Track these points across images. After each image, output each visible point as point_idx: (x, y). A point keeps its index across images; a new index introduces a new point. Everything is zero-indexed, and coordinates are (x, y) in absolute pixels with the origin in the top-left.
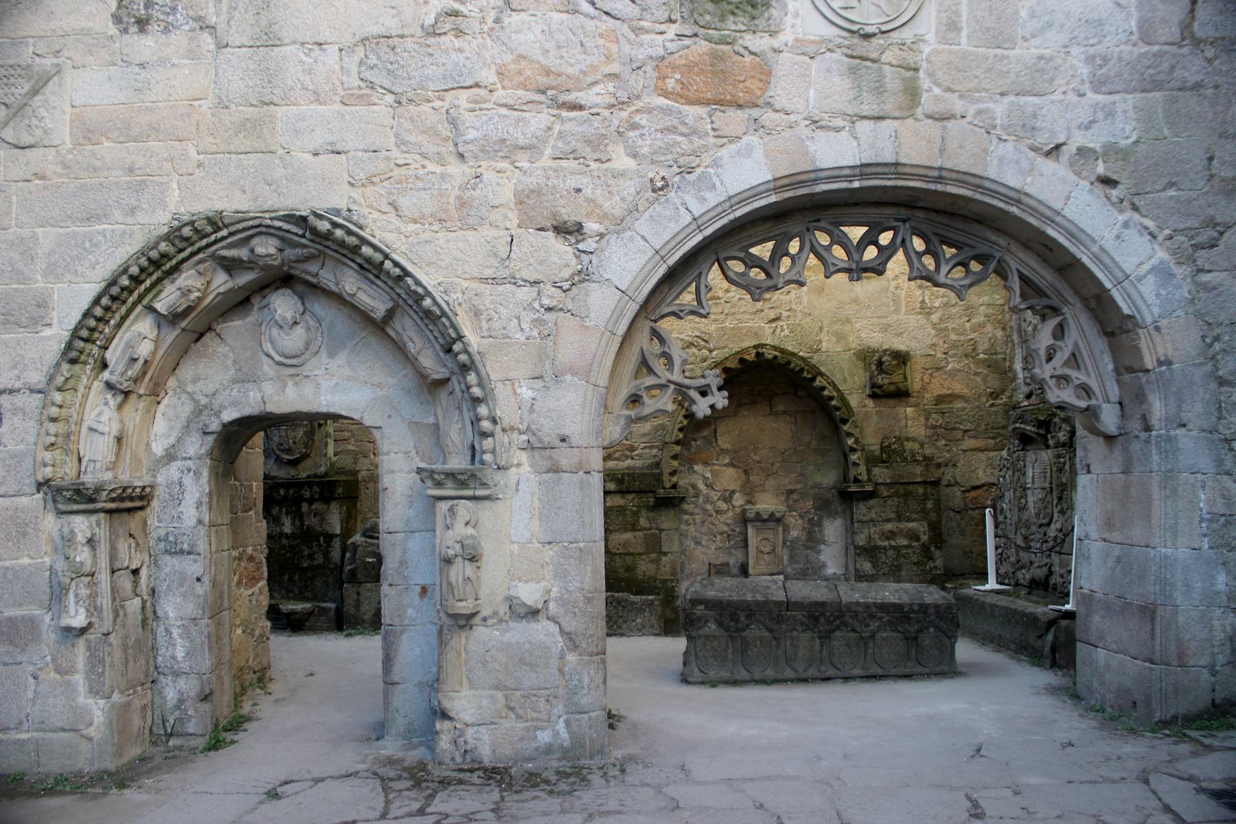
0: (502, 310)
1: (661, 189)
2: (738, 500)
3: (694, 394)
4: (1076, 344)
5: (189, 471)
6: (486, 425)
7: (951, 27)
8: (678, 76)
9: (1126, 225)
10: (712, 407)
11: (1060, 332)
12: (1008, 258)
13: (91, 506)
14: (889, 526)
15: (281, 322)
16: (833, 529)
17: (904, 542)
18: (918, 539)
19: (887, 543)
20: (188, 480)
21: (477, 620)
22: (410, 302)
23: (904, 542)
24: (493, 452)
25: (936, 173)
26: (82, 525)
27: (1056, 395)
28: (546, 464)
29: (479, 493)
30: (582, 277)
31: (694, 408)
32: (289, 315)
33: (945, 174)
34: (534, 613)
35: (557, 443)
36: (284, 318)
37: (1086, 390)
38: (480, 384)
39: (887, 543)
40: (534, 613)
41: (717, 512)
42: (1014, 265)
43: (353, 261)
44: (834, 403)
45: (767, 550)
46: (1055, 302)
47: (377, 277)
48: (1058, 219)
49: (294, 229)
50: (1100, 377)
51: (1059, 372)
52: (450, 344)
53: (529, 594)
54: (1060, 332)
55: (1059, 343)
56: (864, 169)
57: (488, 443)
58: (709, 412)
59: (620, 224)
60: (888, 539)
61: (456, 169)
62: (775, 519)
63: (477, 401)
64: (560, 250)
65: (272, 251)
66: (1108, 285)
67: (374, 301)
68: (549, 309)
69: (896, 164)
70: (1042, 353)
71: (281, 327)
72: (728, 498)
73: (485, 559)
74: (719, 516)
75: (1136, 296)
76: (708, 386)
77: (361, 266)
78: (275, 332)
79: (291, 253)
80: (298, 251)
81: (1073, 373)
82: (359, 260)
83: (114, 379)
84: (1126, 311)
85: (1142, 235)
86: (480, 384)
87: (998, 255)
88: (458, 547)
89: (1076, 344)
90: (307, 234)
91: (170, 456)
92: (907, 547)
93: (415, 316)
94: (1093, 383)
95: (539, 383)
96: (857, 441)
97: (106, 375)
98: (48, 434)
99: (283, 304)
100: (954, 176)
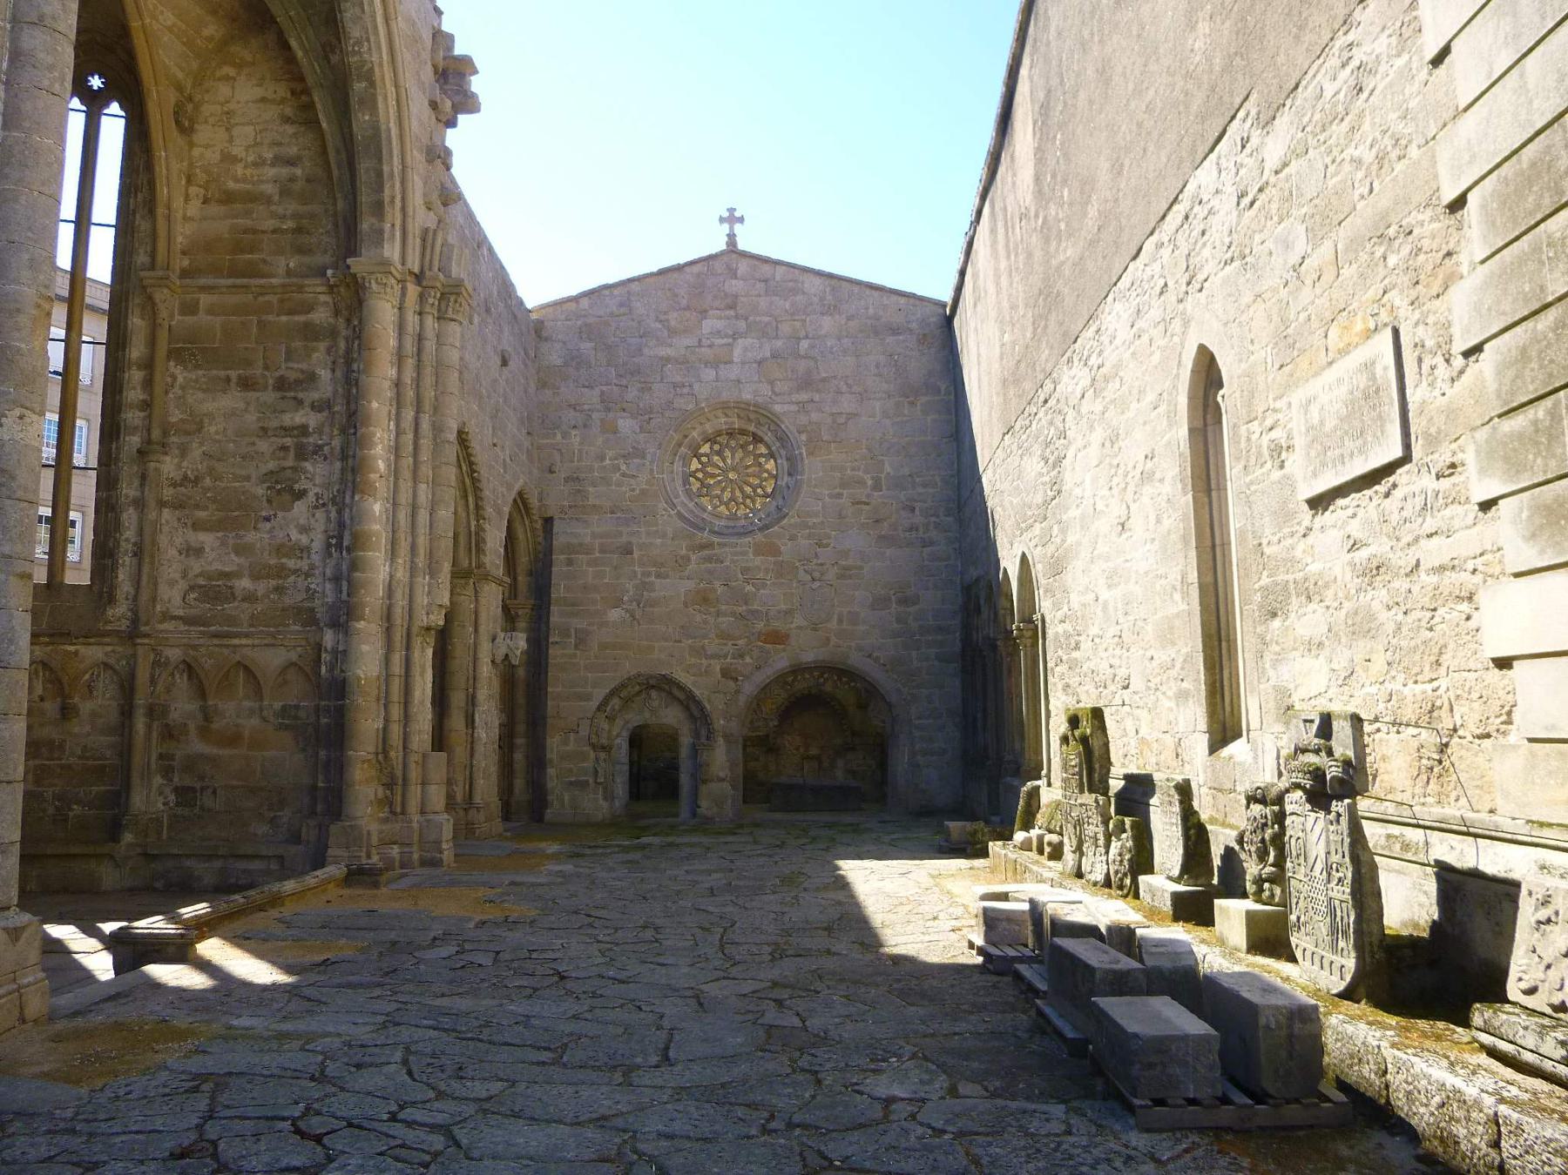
2: (802, 750)
7: (840, 621)
16: (840, 763)
26: (603, 755)
30: (737, 692)
34: (723, 780)
40: (723, 780)
52: (702, 709)
53: (722, 774)
56: (815, 662)
59: (747, 677)
61: (704, 661)
62: (818, 758)
64: (731, 684)
67: (682, 696)
72: (797, 749)
91: (618, 736)
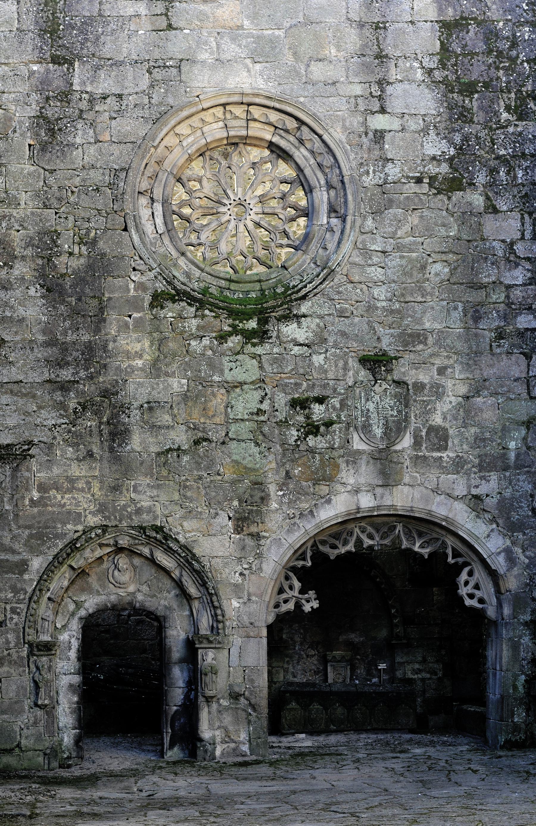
0: (226, 570)
1: (292, 518)
3: (303, 602)
4: (478, 578)
5: (74, 636)
6: (220, 618)
8: (300, 469)
9: (492, 530)
10: (312, 607)
11: (470, 574)
12: (446, 540)
13: (49, 653)
14: (417, 666)
15: (120, 569)
17: (428, 676)
18: (436, 674)
19: (416, 676)
20: (73, 640)
21: (215, 699)
22: (187, 565)
23: (428, 676)
24: (224, 628)
25: (409, 509)
27: (468, 602)
28: (244, 634)
29: (217, 646)
31: (304, 608)
32: (125, 567)
33: (414, 509)
35: (249, 625)
36: (122, 568)
37: (481, 601)
38: (218, 601)
39: (416, 676)
41: (307, 656)
42: (449, 543)
43: (162, 547)
44: (383, 586)
45: (340, 680)
46: (468, 560)
47: (173, 554)
48: (463, 528)
49: (137, 533)
50: (488, 594)
51: (470, 592)
54: (470, 574)
55: (471, 578)
57: (220, 626)
58: (310, 610)
60: (417, 673)
63: (217, 607)
65: (126, 542)
66: (485, 557)
68: (245, 569)
69: (393, 505)
70: (462, 582)
71: (119, 571)
73: (219, 674)
74: (309, 659)
75: (497, 562)
76: (310, 598)
77: (165, 549)
78: (116, 573)
79: (132, 542)
80: (137, 541)
81: (476, 592)
82: (165, 547)
83: (53, 597)
84: (493, 568)
85: (499, 534)
86: (218, 601)
87: (442, 538)
88: (210, 668)
89: (478, 578)
90: (143, 536)
92: (430, 679)
93: (188, 571)
94: (486, 597)
95: (241, 601)
96: (397, 611)
97: (48, 594)
98: (29, 621)
99: (123, 561)
100: (418, 510)
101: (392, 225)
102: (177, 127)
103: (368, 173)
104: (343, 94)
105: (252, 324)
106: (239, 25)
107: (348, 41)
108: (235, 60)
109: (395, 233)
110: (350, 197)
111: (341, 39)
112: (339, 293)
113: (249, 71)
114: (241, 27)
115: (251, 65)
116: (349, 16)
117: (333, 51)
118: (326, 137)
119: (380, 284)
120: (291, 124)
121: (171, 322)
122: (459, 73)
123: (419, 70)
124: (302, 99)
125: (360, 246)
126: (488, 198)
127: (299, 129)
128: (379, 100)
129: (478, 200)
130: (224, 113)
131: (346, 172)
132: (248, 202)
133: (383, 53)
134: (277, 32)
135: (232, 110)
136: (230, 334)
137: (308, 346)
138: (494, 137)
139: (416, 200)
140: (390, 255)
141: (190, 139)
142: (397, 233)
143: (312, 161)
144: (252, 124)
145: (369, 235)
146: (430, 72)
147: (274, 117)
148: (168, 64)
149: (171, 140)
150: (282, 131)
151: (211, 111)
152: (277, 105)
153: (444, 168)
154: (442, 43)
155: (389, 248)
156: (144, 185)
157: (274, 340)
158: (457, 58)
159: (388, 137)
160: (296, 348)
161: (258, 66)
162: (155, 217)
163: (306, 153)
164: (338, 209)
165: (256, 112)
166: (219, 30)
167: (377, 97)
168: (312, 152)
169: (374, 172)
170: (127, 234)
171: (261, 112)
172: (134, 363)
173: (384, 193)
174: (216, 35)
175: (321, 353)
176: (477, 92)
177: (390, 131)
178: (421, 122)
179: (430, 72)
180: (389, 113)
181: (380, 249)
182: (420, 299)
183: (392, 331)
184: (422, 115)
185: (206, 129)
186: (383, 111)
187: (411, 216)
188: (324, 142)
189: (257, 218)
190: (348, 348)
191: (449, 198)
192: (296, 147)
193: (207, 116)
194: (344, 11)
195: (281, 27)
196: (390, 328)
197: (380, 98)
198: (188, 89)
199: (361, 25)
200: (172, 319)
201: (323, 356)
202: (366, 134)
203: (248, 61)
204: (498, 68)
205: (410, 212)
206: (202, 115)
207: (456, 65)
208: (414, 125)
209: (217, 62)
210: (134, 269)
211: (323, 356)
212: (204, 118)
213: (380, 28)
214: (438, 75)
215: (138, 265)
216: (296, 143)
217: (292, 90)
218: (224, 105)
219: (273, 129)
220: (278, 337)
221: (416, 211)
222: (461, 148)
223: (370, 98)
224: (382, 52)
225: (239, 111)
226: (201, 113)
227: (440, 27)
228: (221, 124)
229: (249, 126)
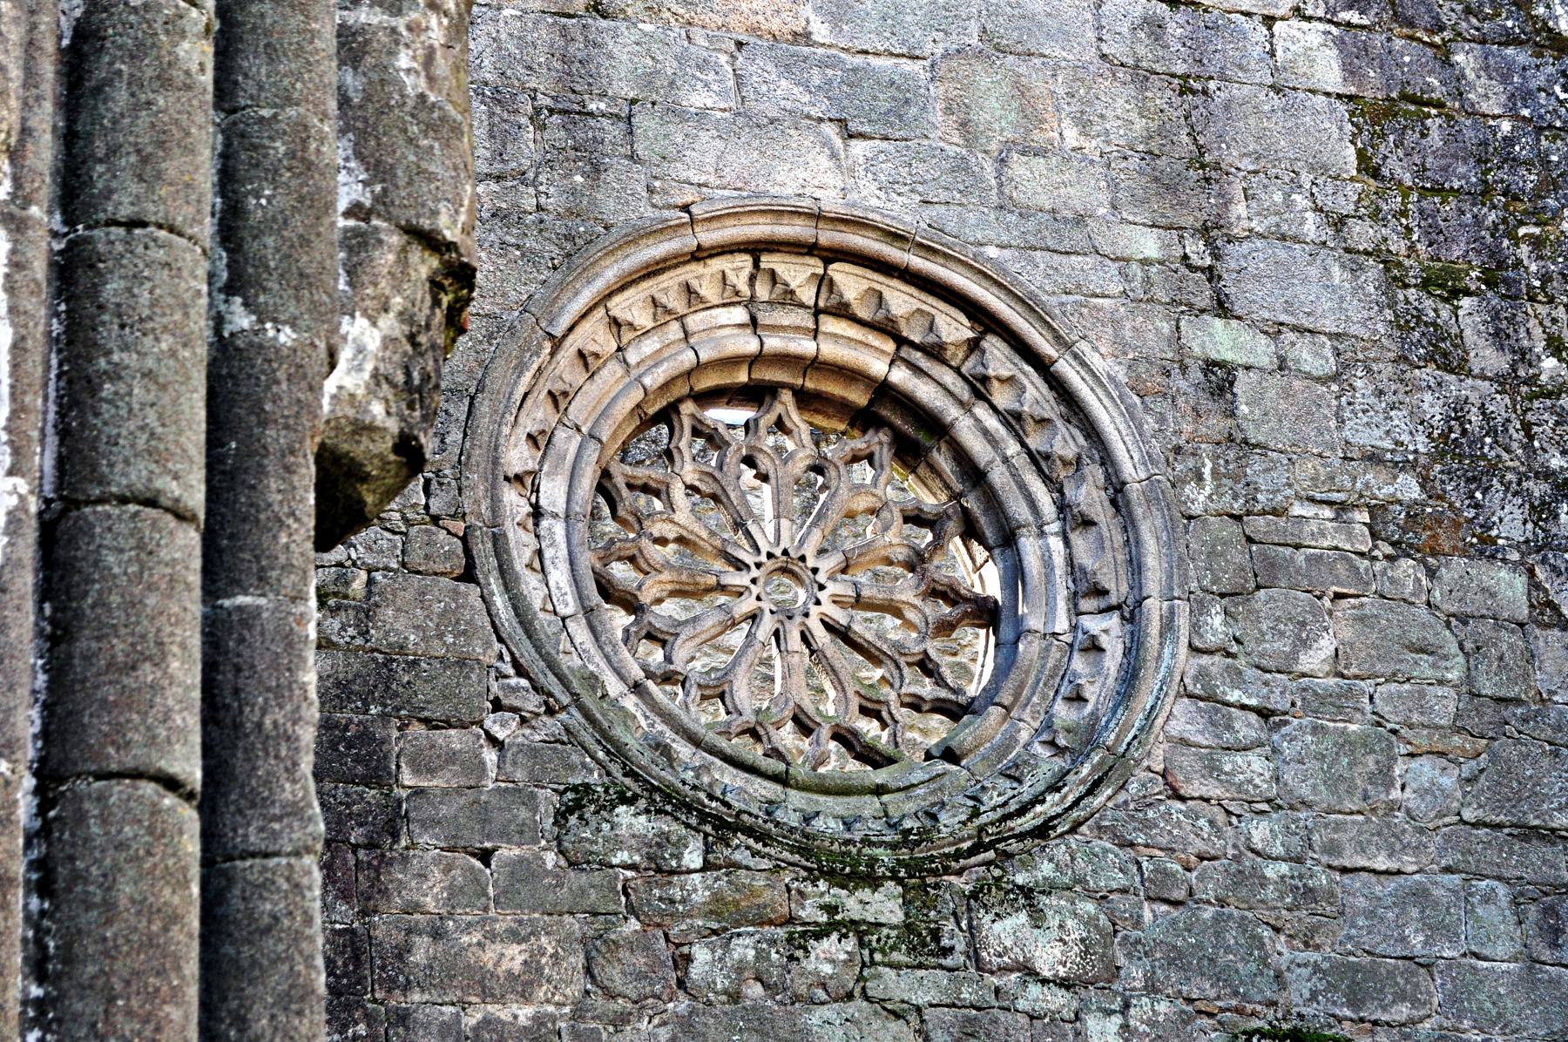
101: (1282, 634)
102: (617, 299)
103: (1199, 478)
104: (1107, 250)
105: (884, 905)
106: (799, 30)
107: (1109, 114)
108: (799, 118)
109: (1293, 657)
110: (1150, 546)
111: (1090, 103)
112: (1148, 825)
113: (834, 156)
114: (803, 37)
115: (838, 142)
116: (1105, 50)
117: (1072, 137)
118: (1066, 368)
119: (1265, 807)
120: (954, 328)
121: (626, 880)
122: (1415, 237)
123: (1310, 215)
124: (992, 252)
125: (1198, 690)
126: (1534, 585)
127: (974, 346)
128: (1210, 280)
129: (1511, 585)
130: (752, 279)
131: (1130, 470)
132: (811, 563)
133: (1208, 158)
134: (908, 66)
135: (780, 269)
136: (821, 933)
137: (1064, 984)
138: (1529, 417)
139: (1341, 568)
140: (1286, 723)
141: (650, 346)
142: (1296, 660)
143: (1012, 448)
144: (830, 325)
145: (1217, 658)
146: (1339, 223)
147: (901, 300)
148: (592, 107)
149: (595, 335)
150: (919, 354)
151: (717, 264)
152: (917, 262)
153: (1409, 488)
154: (1361, 154)
155: (1278, 702)
156: (518, 457)
157: (956, 959)
158: (1405, 196)
159: (1244, 384)
160: (1035, 990)
161: (859, 148)
162: (547, 563)
163: (992, 423)
164: (1107, 582)
165: (851, 283)
166: (743, 38)
167: (1202, 270)
168: (1013, 420)
169: (1215, 473)
170: (473, 592)
171: (865, 285)
172: (504, 1014)
173: (1250, 540)
174: (733, 47)
175: (1109, 1013)
176: (1468, 293)
177: (1248, 368)
178: (1328, 352)
179: (1339, 223)
180: (1239, 318)
181: (1253, 702)
182: (1381, 863)
183: (1314, 956)
184: (1330, 336)
185: (695, 321)
186: (1223, 308)
187: (1330, 613)
188: (1057, 385)
189: (840, 616)
190: (1189, 1001)
191: (1432, 573)
192: (961, 404)
193: (704, 277)
194: (1091, 35)
195: (918, 52)
196: (1307, 944)
197: (1211, 274)
198: (657, 184)
199: (1141, 75)
200: (629, 874)
201: (1117, 1020)
202: (1184, 369)
203: (830, 130)
204: (1516, 241)
205: (1327, 603)
206: (690, 272)
207: (1404, 213)
208: (1313, 358)
209: (740, 121)
210: (497, 705)
211: (1117, 1020)
212: (694, 284)
213: (1194, 92)
214: (1363, 233)
215: (515, 690)
216: (965, 393)
217: (963, 221)
218: (755, 249)
219: (890, 346)
220: (974, 955)
221: (1344, 603)
222: (1444, 436)
223: (1183, 270)
224: (1202, 155)
225: (798, 274)
226: (688, 268)
227: (1352, 114)
228: (739, 315)
229: (823, 328)
